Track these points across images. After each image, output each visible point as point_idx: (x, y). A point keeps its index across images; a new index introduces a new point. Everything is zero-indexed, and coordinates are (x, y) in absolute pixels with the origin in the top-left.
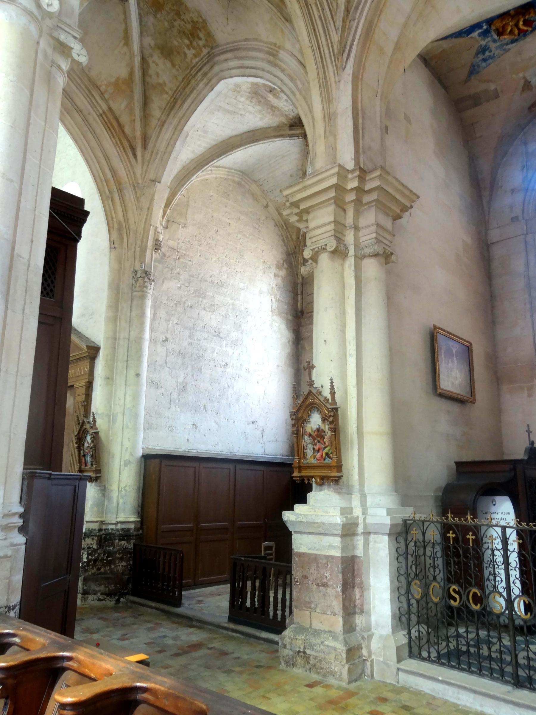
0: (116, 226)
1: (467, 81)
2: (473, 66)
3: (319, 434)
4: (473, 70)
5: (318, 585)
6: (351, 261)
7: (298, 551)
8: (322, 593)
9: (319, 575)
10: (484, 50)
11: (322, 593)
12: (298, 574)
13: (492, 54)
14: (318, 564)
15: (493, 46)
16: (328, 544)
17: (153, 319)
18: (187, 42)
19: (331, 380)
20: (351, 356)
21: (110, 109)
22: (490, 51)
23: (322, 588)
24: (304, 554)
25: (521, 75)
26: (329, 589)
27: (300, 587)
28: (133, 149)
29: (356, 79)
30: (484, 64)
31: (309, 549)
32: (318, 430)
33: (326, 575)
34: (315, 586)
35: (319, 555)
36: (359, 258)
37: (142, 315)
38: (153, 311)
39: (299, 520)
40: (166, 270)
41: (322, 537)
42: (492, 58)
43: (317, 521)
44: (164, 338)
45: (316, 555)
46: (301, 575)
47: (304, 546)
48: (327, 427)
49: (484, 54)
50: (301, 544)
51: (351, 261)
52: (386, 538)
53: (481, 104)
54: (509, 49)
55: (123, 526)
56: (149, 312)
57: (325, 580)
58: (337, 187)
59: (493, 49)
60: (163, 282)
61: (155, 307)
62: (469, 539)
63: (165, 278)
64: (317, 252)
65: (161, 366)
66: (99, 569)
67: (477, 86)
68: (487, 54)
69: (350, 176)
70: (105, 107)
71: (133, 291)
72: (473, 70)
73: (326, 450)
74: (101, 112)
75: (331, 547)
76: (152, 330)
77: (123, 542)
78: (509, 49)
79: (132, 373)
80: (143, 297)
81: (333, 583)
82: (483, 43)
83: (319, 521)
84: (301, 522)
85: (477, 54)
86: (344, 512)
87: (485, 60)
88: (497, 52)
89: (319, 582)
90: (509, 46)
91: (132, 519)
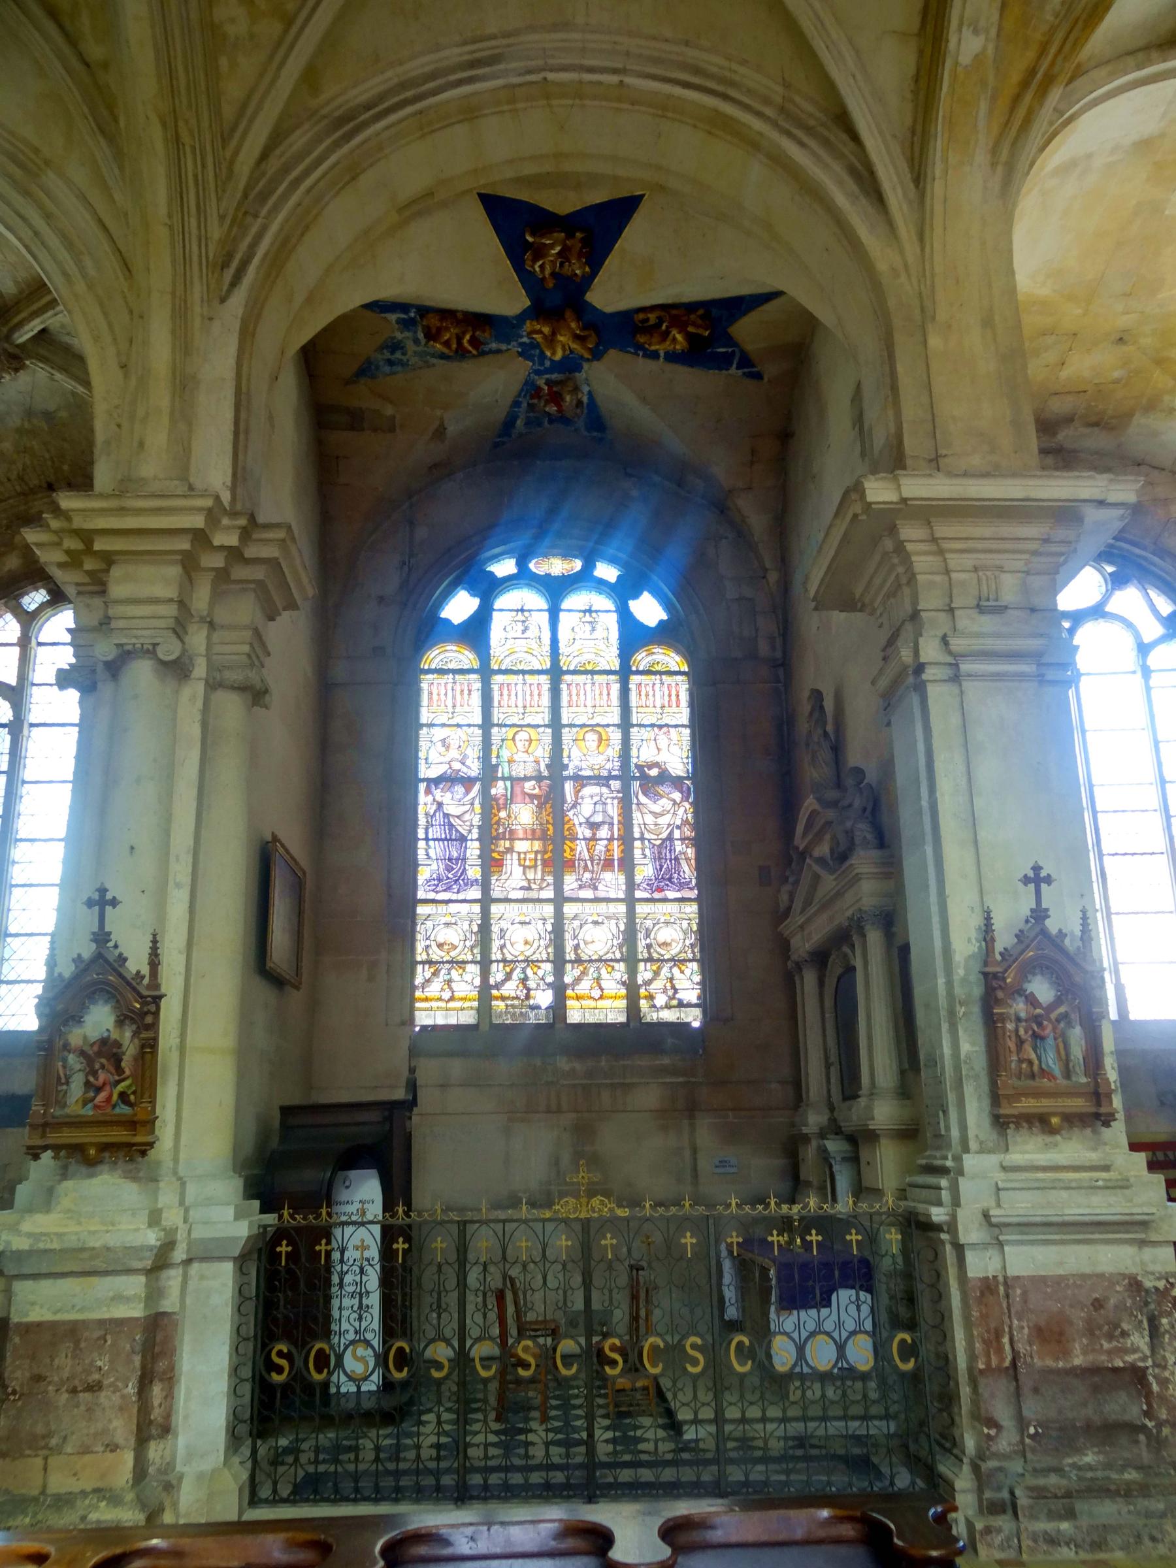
1: (348, 382)
2: (369, 362)
3: (108, 1050)
4: (366, 370)
5: (74, 1391)
6: (194, 690)
7: (25, 1320)
8: (83, 1408)
9: (79, 1369)
10: (395, 346)
11: (83, 1408)
12: (18, 1374)
13: (404, 358)
14: (77, 1343)
15: (411, 347)
16: (111, 1294)
19: (154, 936)
20: (178, 886)
22: (404, 354)
23: (85, 1397)
24: (39, 1324)
25: (439, 413)
26: (103, 1394)
27: (20, 1403)
29: (247, 333)
30: (387, 369)
31: (55, 1313)
32: (104, 1042)
33: (99, 1363)
34: (65, 1396)
35: (84, 1321)
36: (213, 685)
39: (41, 1246)
41: (94, 1280)
42: (402, 365)
43: (91, 1244)
45: (75, 1323)
46: (28, 1375)
47: (42, 1307)
48: (128, 1034)
49: (392, 353)
50: (33, 1304)
51: (194, 690)
52: (229, 1267)
53: (363, 430)
54: (434, 365)
57: (96, 1376)
58: (200, 537)
59: (410, 353)
62: (398, 1249)
64: (129, 652)
67: (362, 397)
68: (398, 355)
69: (225, 521)
72: (366, 370)
73: (121, 1087)
75: (118, 1298)
78: (434, 365)
81: (117, 1379)
82: (399, 336)
83: (97, 1244)
84: (46, 1251)
85: (381, 348)
86: (154, 1219)
87: (390, 363)
88: (414, 360)
89: (77, 1382)
90: (434, 361)
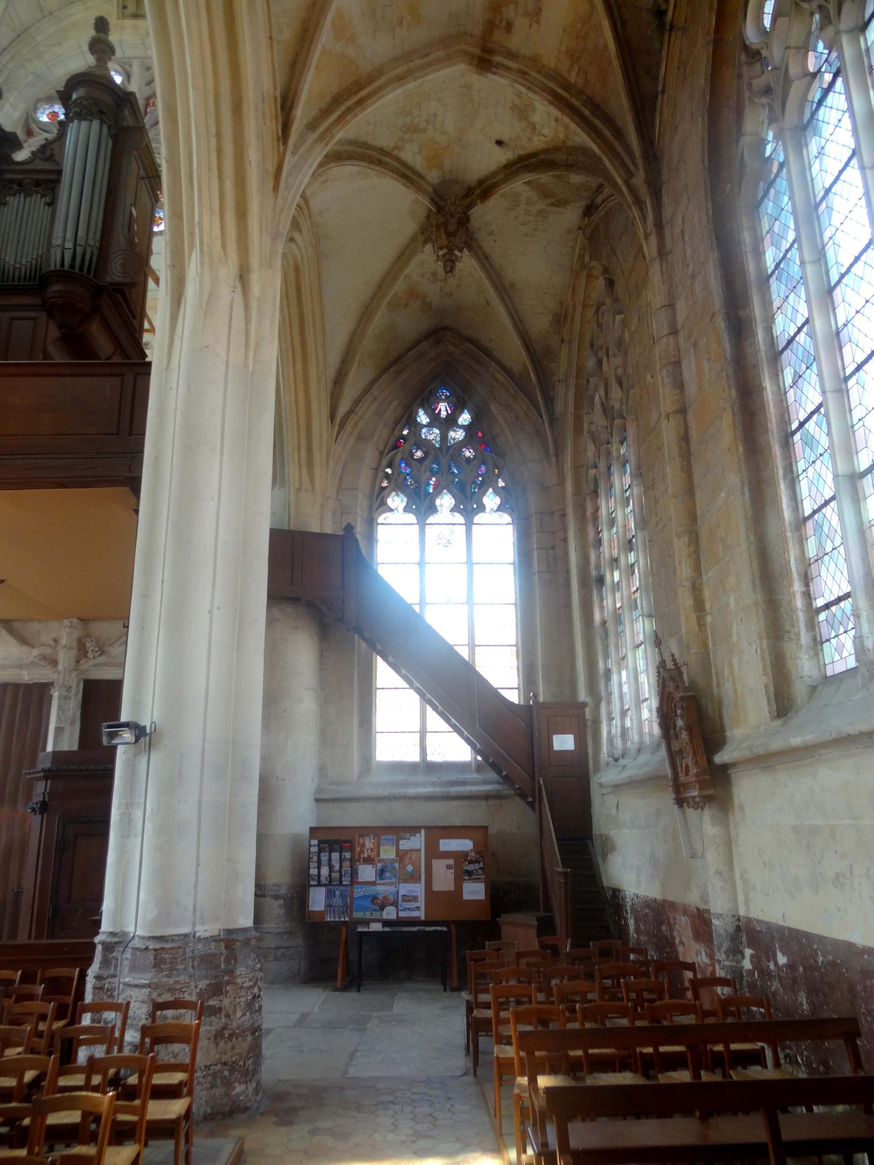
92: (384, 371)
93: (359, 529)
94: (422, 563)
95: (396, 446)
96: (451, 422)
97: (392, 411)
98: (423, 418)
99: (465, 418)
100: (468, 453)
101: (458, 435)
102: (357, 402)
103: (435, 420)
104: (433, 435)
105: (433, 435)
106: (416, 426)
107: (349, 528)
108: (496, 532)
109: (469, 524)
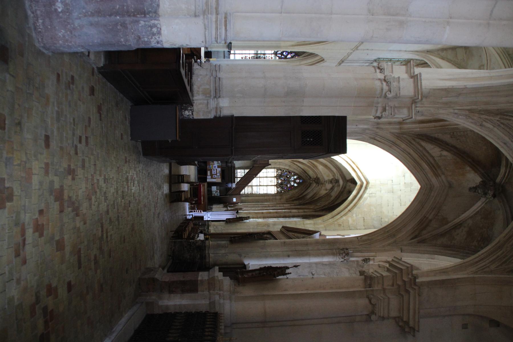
0: (370, 238)
17: (323, 264)
18: (479, 239)
21: (431, 221)
28: (416, 237)
37: (323, 255)
38: (327, 263)
40: (354, 269)
44: (313, 273)
55: (207, 256)
56: (326, 259)
60: (347, 268)
61: (330, 264)
63: (349, 269)
65: (297, 272)
66: (186, 247)
70: (430, 218)
71: (336, 249)
74: (427, 216)
76: (316, 264)
77: (199, 256)
79: (290, 253)
80: (333, 254)
91: (211, 260)
92: (303, 170)
93: (269, 166)
94: (267, 177)
95: (289, 172)
96: (295, 182)
97: (297, 172)
98: (295, 177)
99: (296, 185)
100: (289, 186)
101: (292, 184)
102: (297, 165)
103: (295, 179)
104: (292, 179)
105: (292, 179)
106: (294, 176)
107: (270, 165)
108: (273, 190)
109: (275, 186)
